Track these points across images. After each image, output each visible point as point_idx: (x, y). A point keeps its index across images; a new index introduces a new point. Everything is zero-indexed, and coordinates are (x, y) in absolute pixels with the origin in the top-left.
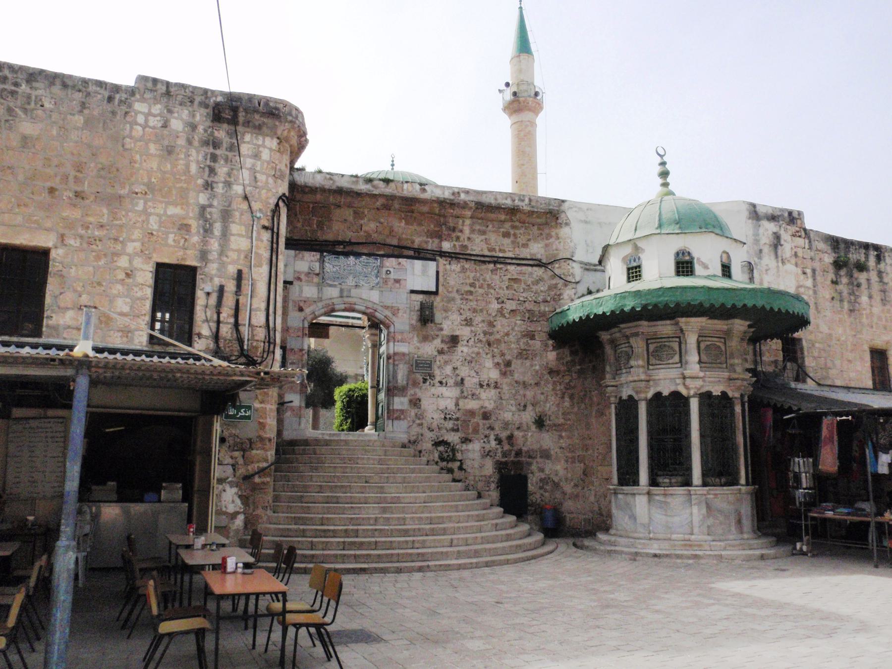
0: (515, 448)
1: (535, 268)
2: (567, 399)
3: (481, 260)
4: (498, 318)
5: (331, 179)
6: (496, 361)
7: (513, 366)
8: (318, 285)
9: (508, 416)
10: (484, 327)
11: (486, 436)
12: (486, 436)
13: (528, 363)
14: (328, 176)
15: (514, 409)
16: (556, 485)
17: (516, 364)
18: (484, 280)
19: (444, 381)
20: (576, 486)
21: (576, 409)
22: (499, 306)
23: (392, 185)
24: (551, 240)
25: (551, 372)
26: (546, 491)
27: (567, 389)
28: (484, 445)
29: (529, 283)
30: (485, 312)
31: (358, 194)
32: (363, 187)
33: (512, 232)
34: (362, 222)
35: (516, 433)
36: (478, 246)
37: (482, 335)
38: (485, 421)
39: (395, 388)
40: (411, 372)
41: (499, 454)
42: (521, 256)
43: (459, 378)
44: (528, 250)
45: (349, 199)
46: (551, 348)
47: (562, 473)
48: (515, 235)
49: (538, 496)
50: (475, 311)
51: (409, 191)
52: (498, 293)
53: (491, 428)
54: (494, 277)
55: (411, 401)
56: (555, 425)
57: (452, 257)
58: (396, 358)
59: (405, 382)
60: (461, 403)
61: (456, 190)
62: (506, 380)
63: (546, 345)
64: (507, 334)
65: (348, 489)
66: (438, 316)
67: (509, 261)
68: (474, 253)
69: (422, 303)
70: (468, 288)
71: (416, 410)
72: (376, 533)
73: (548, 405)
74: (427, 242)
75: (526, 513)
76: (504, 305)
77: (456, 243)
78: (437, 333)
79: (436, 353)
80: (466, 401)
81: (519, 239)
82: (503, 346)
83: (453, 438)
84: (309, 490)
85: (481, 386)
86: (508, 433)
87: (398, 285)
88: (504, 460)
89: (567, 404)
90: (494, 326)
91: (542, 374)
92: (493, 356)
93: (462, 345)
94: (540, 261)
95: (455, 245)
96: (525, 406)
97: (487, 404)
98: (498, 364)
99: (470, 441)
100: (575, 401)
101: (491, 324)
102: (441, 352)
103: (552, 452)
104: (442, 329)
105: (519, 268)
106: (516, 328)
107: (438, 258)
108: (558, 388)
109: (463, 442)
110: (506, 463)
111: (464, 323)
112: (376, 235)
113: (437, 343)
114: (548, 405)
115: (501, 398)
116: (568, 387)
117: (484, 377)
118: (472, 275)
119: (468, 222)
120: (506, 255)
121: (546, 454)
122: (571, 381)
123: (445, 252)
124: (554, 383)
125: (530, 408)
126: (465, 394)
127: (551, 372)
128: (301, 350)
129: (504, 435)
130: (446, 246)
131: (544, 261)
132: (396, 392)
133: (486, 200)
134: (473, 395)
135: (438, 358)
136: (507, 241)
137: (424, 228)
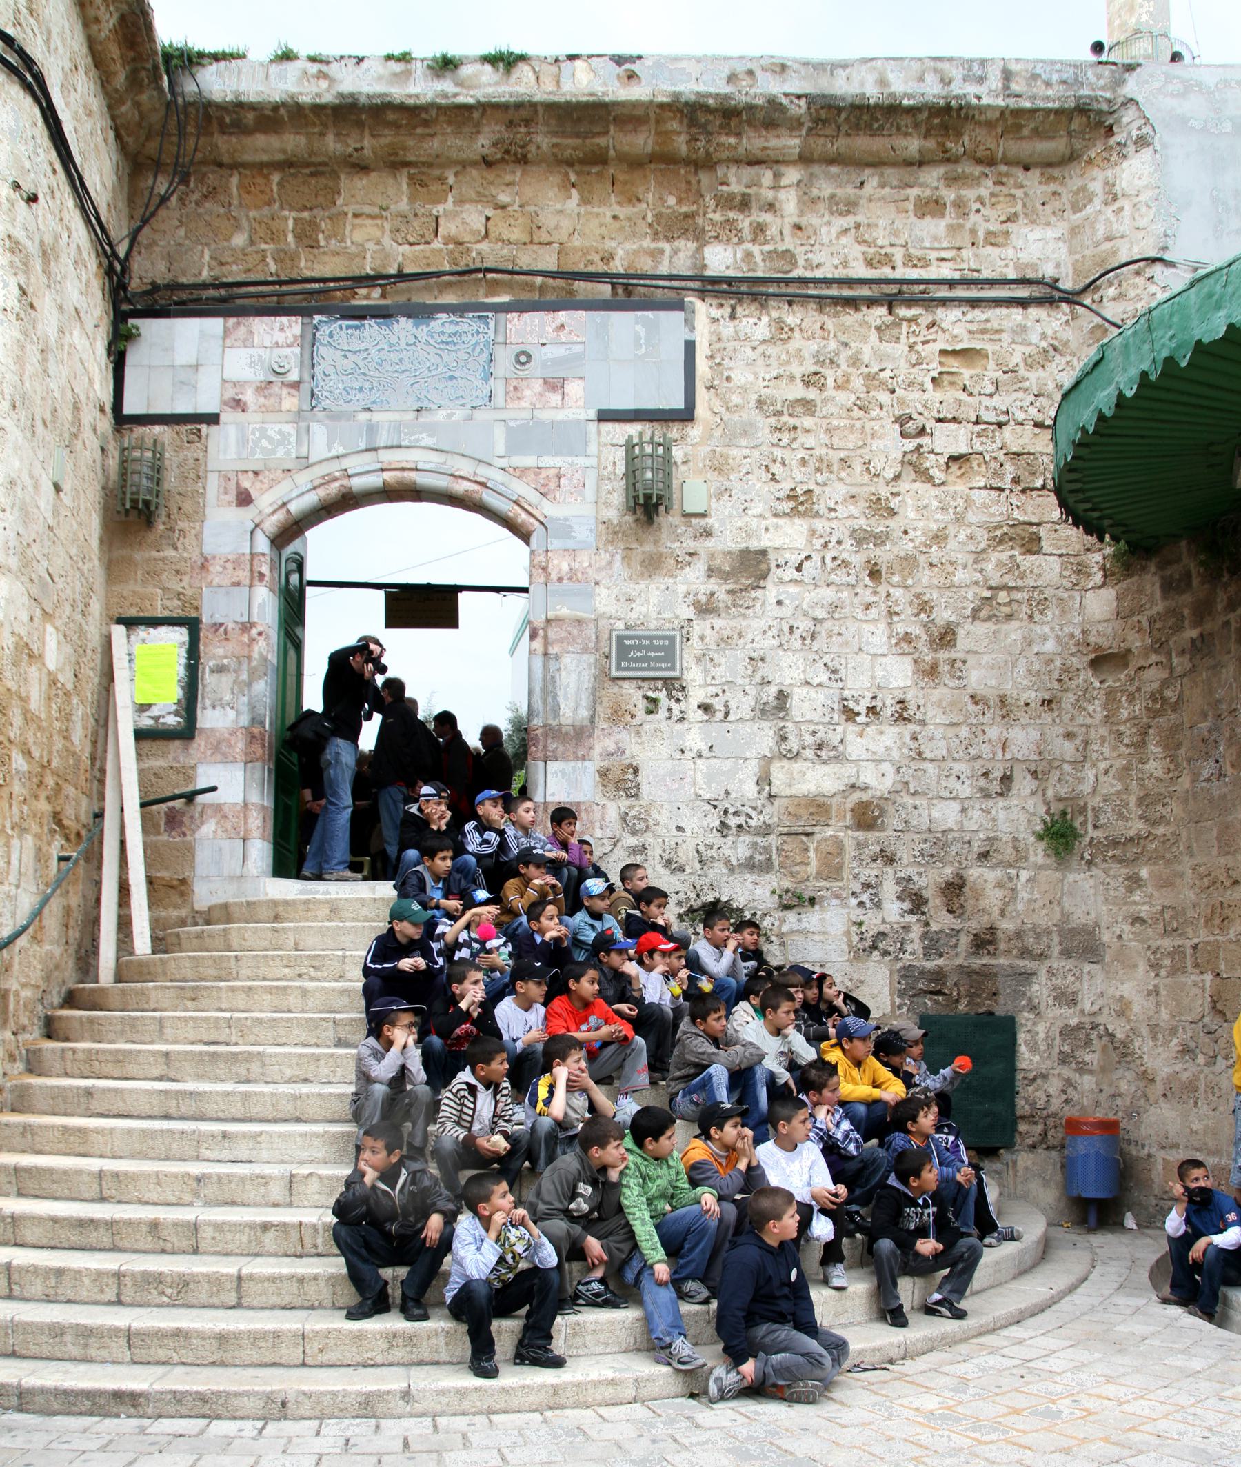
0: (975, 925)
1: (1034, 312)
2: (1153, 749)
3: (842, 296)
4: (904, 486)
5: (322, 75)
6: (901, 629)
7: (963, 642)
8: (299, 416)
9: (946, 815)
10: (856, 516)
11: (867, 886)
12: (867, 886)
13: (1014, 632)
14: (314, 68)
15: (966, 790)
16: (1121, 1051)
17: (971, 636)
18: (855, 362)
19: (718, 704)
20: (1187, 1051)
21: (1185, 782)
22: (909, 445)
23: (523, 70)
24: (1089, 210)
25: (1101, 661)
26: (1083, 1069)
27: (1155, 714)
28: (857, 915)
29: (1017, 359)
30: (858, 467)
31: (413, 116)
32: (422, 88)
33: (949, 195)
34: (438, 209)
35: (975, 873)
36: (833, 252)
37: (848, 543)
38: (861, 835)
39: (555, 732)
40: (605, 678)
41: (915, 945)
42: (986, 274)
43: (773, 690)
44: (1010, 252)
45: (388, 138)
46: (1098, 578)
47: (1140, 1006)
48: (959, 205)
49: (1054, 1086)
50: (823, 465)
51: (581, 84)
52: (901, 402)
53: (891, 860)
54: (886, 347)
55: (603, 774)
56: (1115, 843)
57: (740, 296)
58: (552, 634)
59: (584, 713)
60: (779, 773)
61: (741, 68)
62: (936, 694)
63: (1081, 570)
64: (939, 538)
65: (256, 1068)
66: (693, 490)
67: (943, 292)
68: (818, 274)
69: (630, 446)
70: (798, 391)
71: (624, 803)
72: (269, 1238)
73: (1090, 774)
74: (656, 254)
75: (1010, 1146)
76: (924, 440)
77: (755, 249)
78: (690, 545)
79: (689, 613)
80: (797, 766)
81: (974, 218)
82: (925, 577)
83: (750, 893)
84: (132, 1069)
85: (850, 715)
86: (949, 871)
87: (555, 398)
88: (930, 965)
89: (1155, 767)
90: (892, 513)
91: (1065, 669)
92: (891, 614)
93: (781, 582)
94: (1053, 284)
95: (749, 255)
96: (1007, 779)
97: (868, 776)
98: (907, 638)
99: (812, 901)
100: (1182, 752)
101: (881, 508)
102: (706, 609)
103: (1106, 937)
104: (708, 533)
105: (977, 314)
106: (971, 517)
107: (690, 299)
108: (1124, 713)
109: (786, 907)
110: (938, 975)
111: (787, 506)
112: (484, 246)
113: (693, 579)
114: (1090, 774)
115: (920, 754)
116: (1159, 703)
117: (858, 686)
118: (813, 346)
119: (792, 175)
120: (934, 272)
121: (1084, 945)
122: (1165, 684)
123: (715, 281)
124: (1110, 693)
125: (1024, 785)
126: (793, 744)
127: (1101, 661)
128: (247, 627)
129: (930, 880)
130: (720, 259)
131: (1067, 284)
132: (552, 745)
133: (844, 87)
134: (820, 747)
135: (697, 628)
136: (932, 229)
137: (647, 209)
